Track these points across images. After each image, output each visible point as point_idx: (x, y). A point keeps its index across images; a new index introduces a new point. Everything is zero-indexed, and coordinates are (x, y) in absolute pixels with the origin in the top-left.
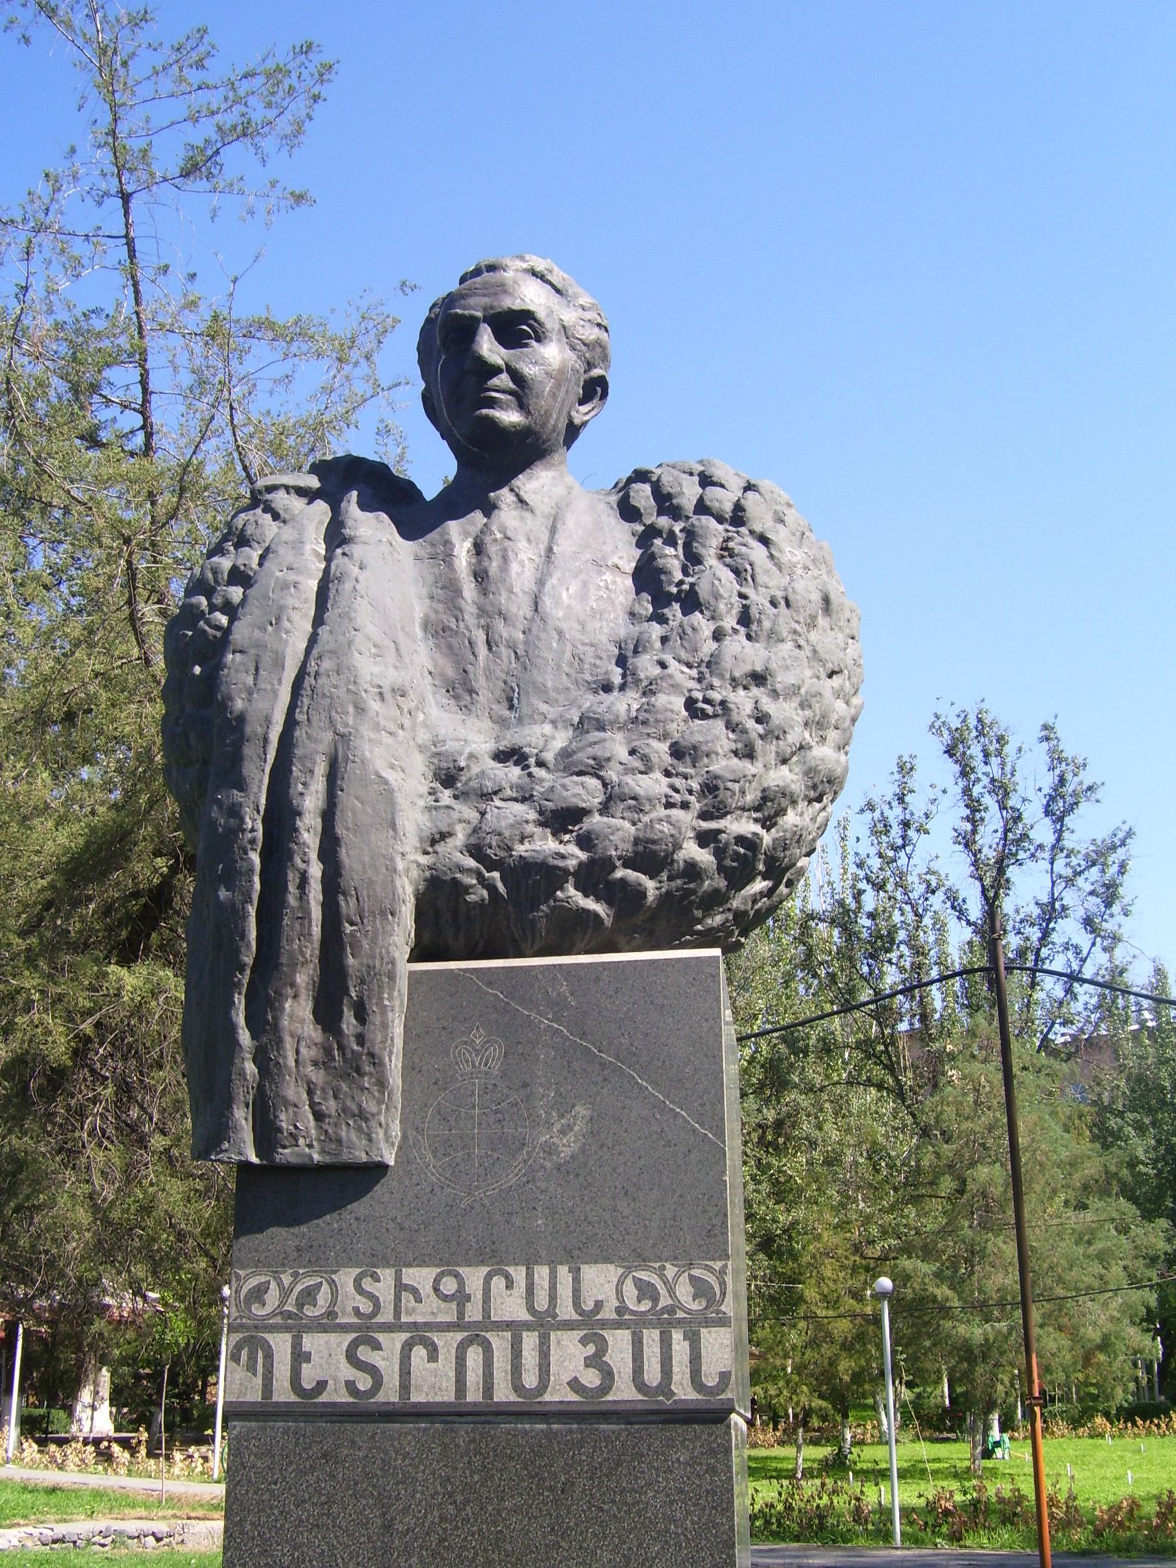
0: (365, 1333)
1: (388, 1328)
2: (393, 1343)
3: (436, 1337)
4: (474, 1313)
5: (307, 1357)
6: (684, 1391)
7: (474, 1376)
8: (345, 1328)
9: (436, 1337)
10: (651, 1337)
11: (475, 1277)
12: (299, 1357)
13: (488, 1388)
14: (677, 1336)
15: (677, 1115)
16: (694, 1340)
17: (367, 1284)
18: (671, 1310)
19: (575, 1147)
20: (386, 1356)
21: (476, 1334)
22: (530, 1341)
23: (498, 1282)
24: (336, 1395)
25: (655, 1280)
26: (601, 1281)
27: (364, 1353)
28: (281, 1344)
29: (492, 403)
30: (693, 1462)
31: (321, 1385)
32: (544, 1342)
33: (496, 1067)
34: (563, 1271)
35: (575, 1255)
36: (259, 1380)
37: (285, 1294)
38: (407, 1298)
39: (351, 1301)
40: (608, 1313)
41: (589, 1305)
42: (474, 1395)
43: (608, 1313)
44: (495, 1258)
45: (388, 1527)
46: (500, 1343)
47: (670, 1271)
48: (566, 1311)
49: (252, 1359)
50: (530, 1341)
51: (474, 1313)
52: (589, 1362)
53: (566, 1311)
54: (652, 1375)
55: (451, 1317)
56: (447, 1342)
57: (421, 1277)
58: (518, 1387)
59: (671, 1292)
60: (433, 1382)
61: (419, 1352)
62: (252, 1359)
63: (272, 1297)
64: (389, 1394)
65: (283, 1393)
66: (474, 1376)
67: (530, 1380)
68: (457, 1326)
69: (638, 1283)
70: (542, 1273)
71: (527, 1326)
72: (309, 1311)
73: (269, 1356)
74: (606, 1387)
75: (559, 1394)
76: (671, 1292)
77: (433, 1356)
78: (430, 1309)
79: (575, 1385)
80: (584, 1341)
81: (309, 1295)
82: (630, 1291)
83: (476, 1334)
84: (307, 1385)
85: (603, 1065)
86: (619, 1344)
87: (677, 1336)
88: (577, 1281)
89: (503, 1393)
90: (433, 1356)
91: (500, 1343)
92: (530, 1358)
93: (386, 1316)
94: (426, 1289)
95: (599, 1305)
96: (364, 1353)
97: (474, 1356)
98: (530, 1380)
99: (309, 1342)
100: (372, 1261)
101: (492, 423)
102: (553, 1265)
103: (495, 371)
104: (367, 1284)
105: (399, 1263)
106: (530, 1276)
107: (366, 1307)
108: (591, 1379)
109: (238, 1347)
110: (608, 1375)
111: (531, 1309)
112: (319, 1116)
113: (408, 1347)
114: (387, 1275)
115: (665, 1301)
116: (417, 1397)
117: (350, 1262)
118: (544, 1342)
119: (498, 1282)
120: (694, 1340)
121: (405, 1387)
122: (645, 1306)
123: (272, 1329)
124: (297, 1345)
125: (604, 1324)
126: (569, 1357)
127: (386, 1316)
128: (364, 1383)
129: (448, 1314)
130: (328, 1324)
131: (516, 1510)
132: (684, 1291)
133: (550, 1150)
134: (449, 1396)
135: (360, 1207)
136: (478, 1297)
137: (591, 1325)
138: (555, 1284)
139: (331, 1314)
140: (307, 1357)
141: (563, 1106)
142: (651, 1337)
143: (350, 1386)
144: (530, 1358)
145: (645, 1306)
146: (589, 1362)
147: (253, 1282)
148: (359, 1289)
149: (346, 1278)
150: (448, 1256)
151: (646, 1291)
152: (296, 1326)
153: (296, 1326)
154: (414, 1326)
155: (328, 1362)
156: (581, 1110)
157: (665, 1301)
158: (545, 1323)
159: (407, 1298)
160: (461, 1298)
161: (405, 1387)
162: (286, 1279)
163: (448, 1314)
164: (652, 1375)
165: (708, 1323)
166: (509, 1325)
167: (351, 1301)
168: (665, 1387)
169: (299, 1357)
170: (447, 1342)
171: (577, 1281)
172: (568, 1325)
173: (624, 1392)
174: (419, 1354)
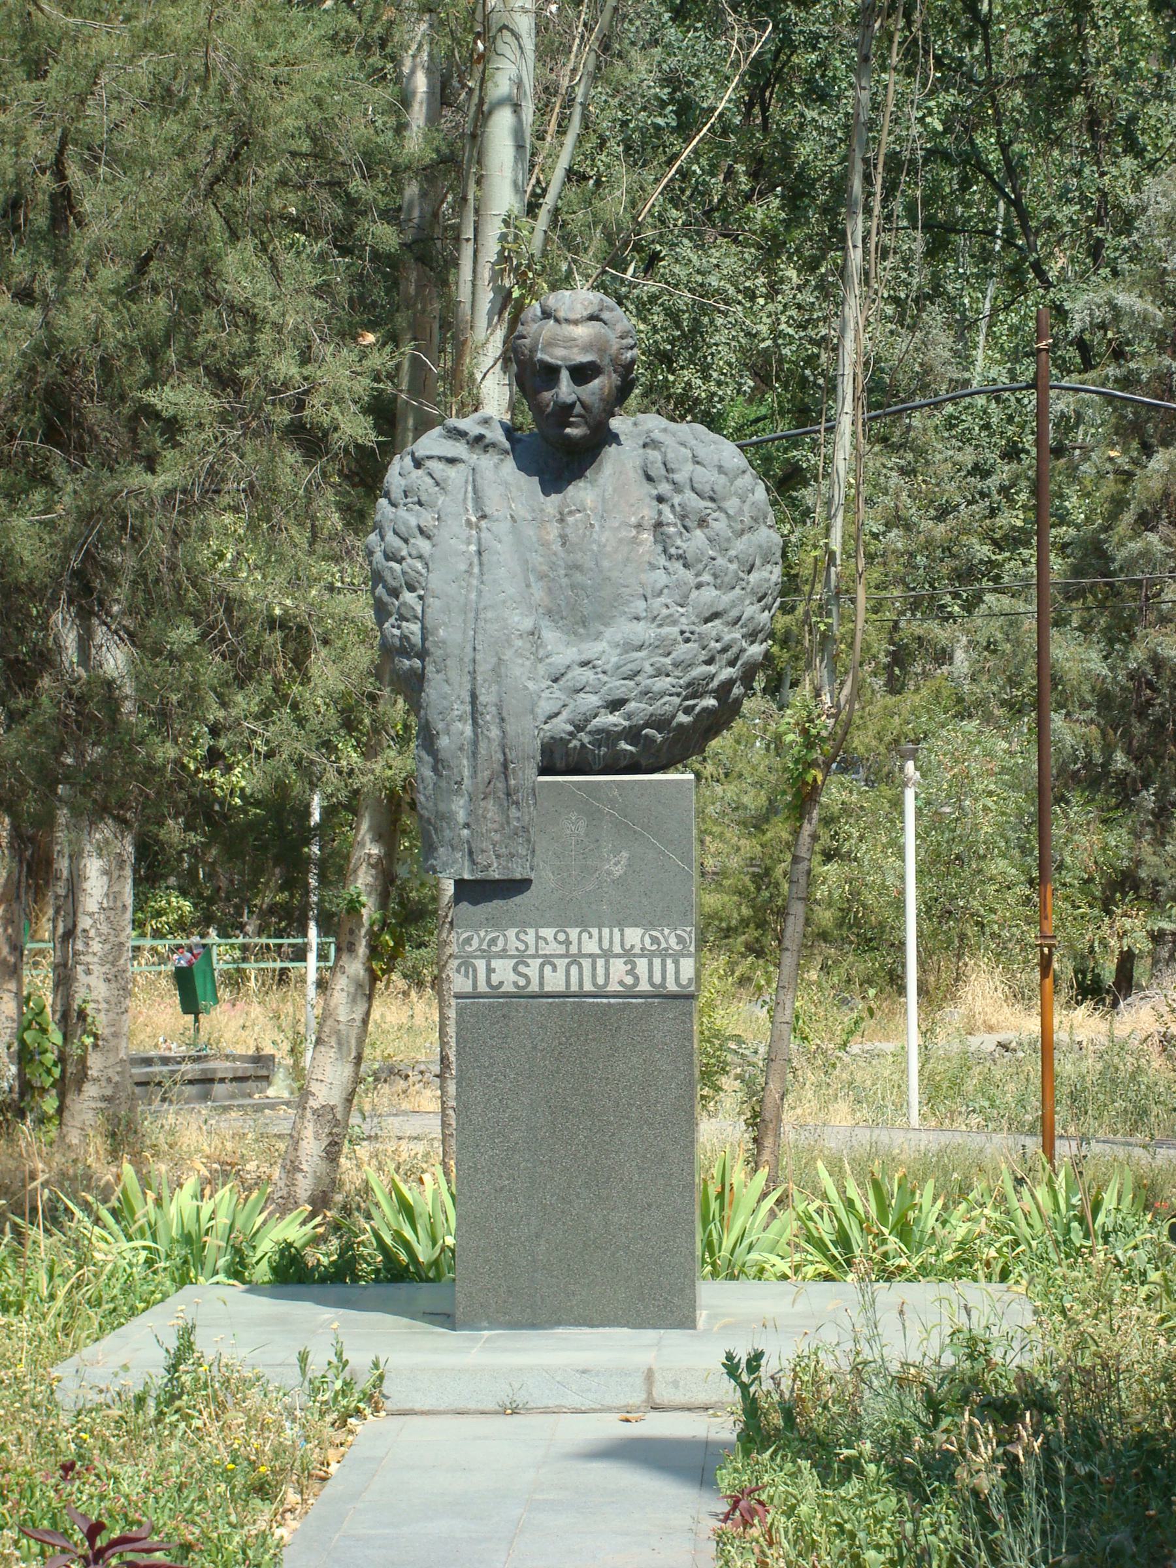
0: (521, 959)
1: (534, 957)
2: (535, 963)
3: (555, 961)
4: (574, 949)
5: (494, 971)
6: (671, 987)
8: (511, 957)
9: (555, 961)
10: (657, 962)
11: (574, 933)
12: (490, 971)
13: (581, 985)
14: (669, 961)
17: (522, 936)
18: (666, 949)
20: (532, 970)
21: (575, 960)
22: (600, 963)
23: (585, 936)
24: (508, 988)
25: (658, 934)
26: (634, 936)
27: (522, 968)
28: (481, 965)
29: (571, 425)
30: (674, 1019)
31: (501, 983)
32: (607, 963)
33: (582, 832)
34: (616, 930)
35: (621, 924)
36: (470, 982)
37: (482, 941)
38: (541, 943)
39: (514, 944)
40: (637, 950)
41: (628, 947)
42: (574, 988)
43: (637, 950)
44: (583, 924)
45: (535, 1048)
47: (666, 931)
48: (617, 949)
49: (467, 972)
50: (600, 963)
51: (574, 949)
52: (628, 973)
53: (617, 949)
54: (657, 979)
55: (563, 952)
56: (561, 963)
57: (548, 933)
58: (595, 984)
59: (667, 941)
60: (555, 981)
61: (548, 968)
62: (467, 972)
63: (475, 942)
64: (534, 987)
65: (483, 987)
67: (601, 981)
68: (566, 956)
69: (651, 936)
70: (606, 931)
71: (598, 956)
72: (494, 949)
73: (475, 970)
74: (635, 985)
75: (614, 987)
76: (667, 941)
77: (555, 969)
78: (553, 948)
79: (621, 983)
80: (625, 963)
81: (493, 941)
82: (647, 940)
83: (575, 960)
84: (494, 983)
86: (642, 965)
87: (669, 961)
88: (622, 935)
89: (588, 987)
90: (555, 969)
91: (586, 964)
92: (600, 971)
93: (532, 951)
94: (550, 938)
95: (633, 946)
96: (522, 968)
97: (574, 970)
98: (601, 981)
99: (494, 963)
100: (523, 925)
101: (568, 436)
102: (611, 927)
103: (573, 405)
104: (522, 936)
105: (537, 926)
106: (600, 933)
107: (522, 947)
108: (629, 980)
109: (459, 966)
110: (637, 978)
111: (601, 948)
112: (498, 856)
113: (542, 965)
114: (531, 931)
115: (664, 945)
116: (547, 989)
117: (513, 926)
118: (607, 963)
119: (585, 936)
121: (541, 984)
122: (655, 947)
123: (476, 957)
124: (488, 965)
125: (635, 955)
126: (618, 968)
128: (522, 982)
129: (561, 950)
130: (503, 954)
131: (594, 1039)
132: (673, 941)
133: (609, 873)
134: (562, 988)
135: (518, 899)
136: (575, 942)
137: (628, 955)
138: (612, 937)
139: (504, 950)
140: (494, 971)
141: (616, 852)
142: (657, 962)
143: (515, 984)
144: (600, 971)
145: (655, 947)
146: (628, 973)
147: (465, 935)
148: (518, 938)
149: (511, 933)
150: (561, 923)
151: (655, 940)
152: (488, 956)
153: (488, 956)
154: (545, 956)
155: (504, 974)
156: (625, 854)
157: (664, 945)
158: (607, 955)
159: (541, 943)
160: (568, 943)
161: (541, 984)
162: (482, 934)
163: (561, 950)
164: (657, 979)
165: (683, 956)
166: (590, 955)
167: (514, 944)
168: (663, 984)
169: (490, 971)
170: (561, 963)
171: (622, 935)
172: (618, 956)
173: (644, 986)
174: (548, 968)
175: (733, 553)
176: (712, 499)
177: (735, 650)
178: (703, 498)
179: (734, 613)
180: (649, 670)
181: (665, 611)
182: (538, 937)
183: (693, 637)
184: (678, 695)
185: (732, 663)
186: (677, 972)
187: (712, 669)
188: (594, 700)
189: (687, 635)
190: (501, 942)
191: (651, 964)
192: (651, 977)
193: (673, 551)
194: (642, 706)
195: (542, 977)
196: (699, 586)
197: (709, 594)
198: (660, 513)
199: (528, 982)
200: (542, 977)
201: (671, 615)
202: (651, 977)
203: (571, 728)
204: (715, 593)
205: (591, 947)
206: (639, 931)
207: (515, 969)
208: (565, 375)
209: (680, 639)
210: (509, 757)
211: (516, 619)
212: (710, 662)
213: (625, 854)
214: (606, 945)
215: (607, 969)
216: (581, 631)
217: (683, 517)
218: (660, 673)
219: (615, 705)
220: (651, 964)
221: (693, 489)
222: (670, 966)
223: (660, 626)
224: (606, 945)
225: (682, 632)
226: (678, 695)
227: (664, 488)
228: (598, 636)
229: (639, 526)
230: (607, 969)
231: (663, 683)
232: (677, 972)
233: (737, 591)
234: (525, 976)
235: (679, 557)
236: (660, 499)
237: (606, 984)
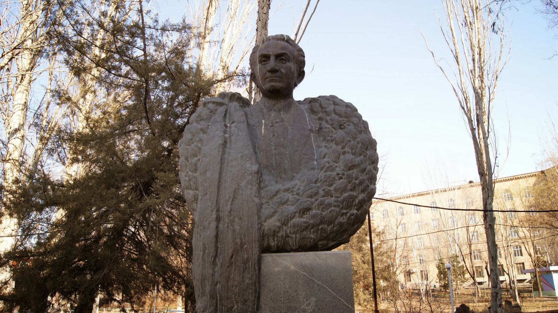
15: (340, 300)
19: (311, 310)
85: (318, 285)
175: (358, 140)
176: (346, 117)
177: (365, 184)
178: (341, 117)
179: (363, 166)
180: (321, 192)
181: (327, 165)
183: (344, 177)
184: (338, 206)
185: (363, 191)
187: (354, 193)
188: (292, 209)
189: (340, 175)
193: (329, 138)
194: (319, 212)
196: (344, 153)
197: (349, 157)
198: (320, 124)
201: (331, 166)
203: (278, 224)
204: (352, 156)
208: (272, 58)
209: (337, 178)
210: (244, 241)
211: (248, 166)
212: (353, 190)
213: (314, 299)
216: (284, 176)
217: (332, 125)
218: (328, 194)
219: (304, 211)
221: (336, 113)
223: (325, 172)
225: (338, 174)
226: (338, 206)
227: (320, 115)
228: (292, 178)
229: (311, 130)
231: (332, 200)
233: (362, 157)
235: (332, 141)
236: (320, 119)
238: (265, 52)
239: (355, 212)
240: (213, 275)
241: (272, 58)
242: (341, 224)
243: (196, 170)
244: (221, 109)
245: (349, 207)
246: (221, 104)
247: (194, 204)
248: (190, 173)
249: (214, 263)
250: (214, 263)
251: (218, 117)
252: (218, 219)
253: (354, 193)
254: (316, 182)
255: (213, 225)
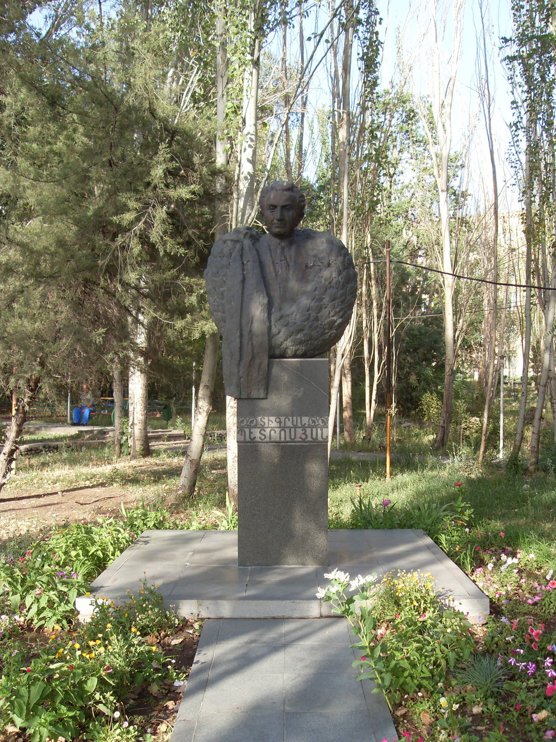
7: (283, 436)
8: (259, 428)
11: (283, 419)
12: (251, 433)
14: (319, 429)
16: (322, 430)
22: (293, 430)
23: (287, 420)
26: (305, 420)
27: (263, 432)
28: (247, 431)
37: (247, 421)
38: (270, 422)
40: (307, 425)
42: (283, 439)
43: (307, 425)
46: (287, 430)
48: (299, 425)
50: (293, 430)
51: (283, 425)
53: (299, 425)
54: (314, 436)
56: (278, 430)
58: (291, 438)
61: (273, 432)
63: (245, 422)
65: (248, 439)
66: (283, 436)
67: (293, 437)
70: (295, 418)
73: (245, 433)
74: (306, 438)
75: (298, 439)
79: (301, 438)
81: (252, 422)
82: (311, 421)
86: (309, 431)
89: (288, 439)
92: (293, 433)
96: (263, 432)
98: (293, 437)
108: (304, 437)
110: (307, 436)
113: (271, 431)
114: (266, 418)
119: (287, 420)
120: (322, 430)
121: (270, 438)
127: (266, 425)
132: (320, 422)
134: (278, 440)
137: (303, 427)
142: (314, 430)
143: (260, 438)
144: (293, 433)
152: (250, 427)
153: (250, 427)
156: (302, 389)
158: (295, 427)
159: (270, 422)
161: (270, 438)
168: (317, 438)
169: (251, 433)
172: (299, 427)
173: (309, 439)
174: (273, 432)
182: (269, 420)
186: (322, 433)
190: (255, 421)
191: (312, 431)
192: (312, 435)
195: (270, 435)
199: (265, 437)
200: (270, 435)
202: (312, 435)
205: (289, 424)
206: (308, 418)
207: (260, 433)
214: (295, 423)
215: (295, 432)
220: (312, 431)
222: (319, 431)
224: (295, 423)
230: (295, 432)
232: (322, 433)
234: (264, 435)
237: (295, 438)
238: (275, 204)
239: (334, 331)
240: (238, 372)
241: (279, 208)
242: (324, 340)
243: (222, 299)
244: (238, 246)
245: (331, 328)
246: (237, 241)
247: (222, 323)
248: (218, 300)
249: (239, 365)
250: (239, 365)
251: (235, 254)
252: (241, 336)
253: (335, 318)
254: (308, 311)
255: (238, 340)
